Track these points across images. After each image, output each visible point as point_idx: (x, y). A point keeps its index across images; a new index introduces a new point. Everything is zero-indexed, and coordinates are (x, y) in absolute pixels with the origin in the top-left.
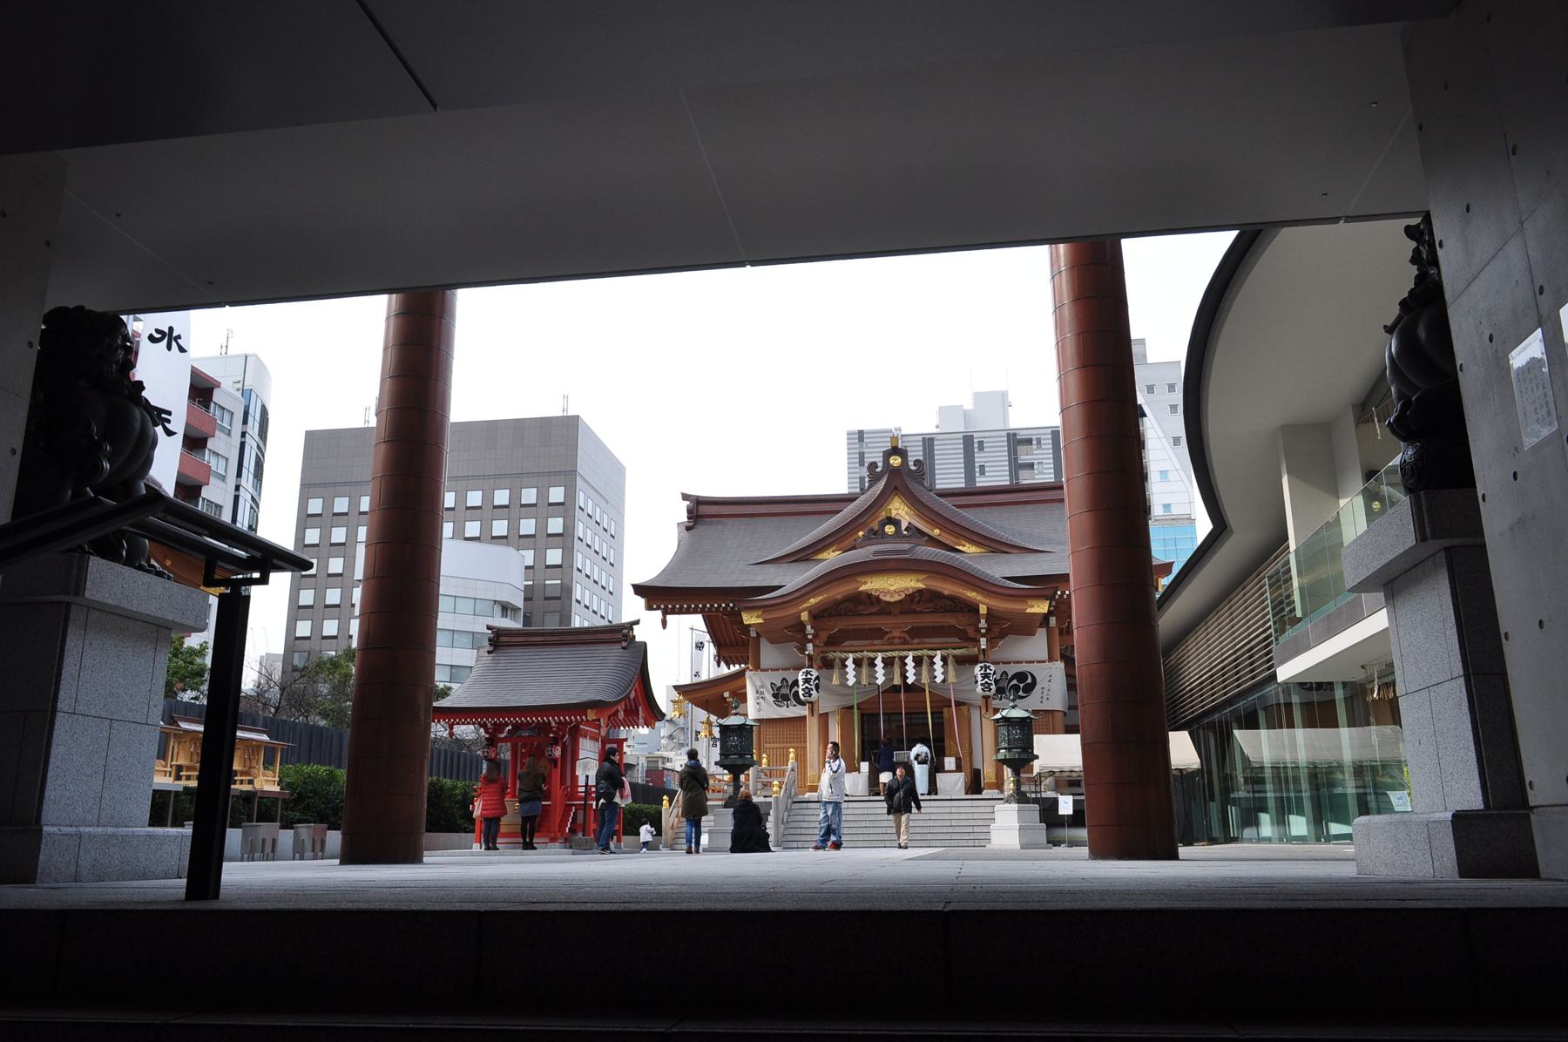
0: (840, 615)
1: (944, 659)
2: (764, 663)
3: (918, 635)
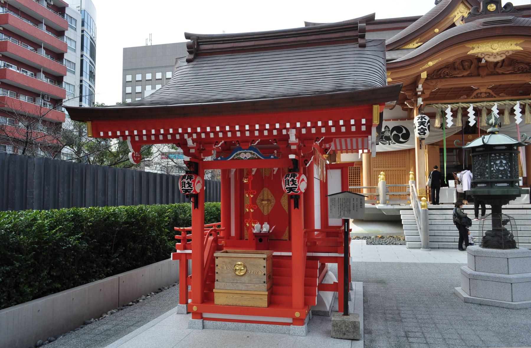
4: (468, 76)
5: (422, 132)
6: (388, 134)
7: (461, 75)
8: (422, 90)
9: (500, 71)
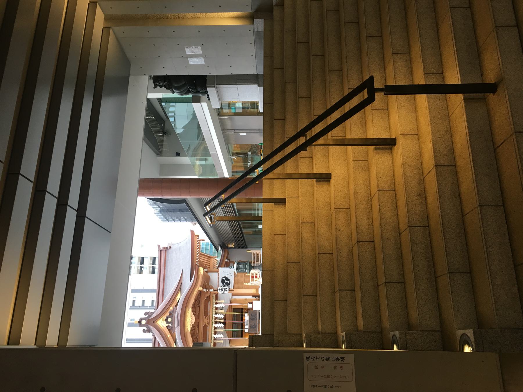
1: (216, 303)
3: (206, 314)
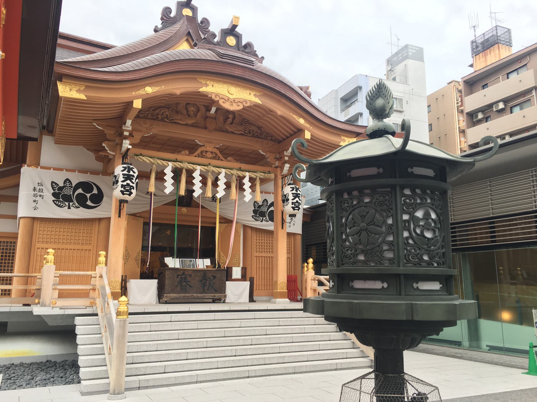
0: (157, 119)
1: (251, 180)
2: (45, 159)
3: (226, 153)
4: (192, 125)
5: (127, 191)
6: (68, 192)
7: (184, 123)
8: (130, 129)
9: (230, 129)
